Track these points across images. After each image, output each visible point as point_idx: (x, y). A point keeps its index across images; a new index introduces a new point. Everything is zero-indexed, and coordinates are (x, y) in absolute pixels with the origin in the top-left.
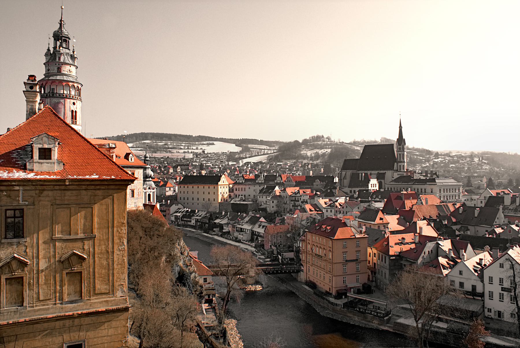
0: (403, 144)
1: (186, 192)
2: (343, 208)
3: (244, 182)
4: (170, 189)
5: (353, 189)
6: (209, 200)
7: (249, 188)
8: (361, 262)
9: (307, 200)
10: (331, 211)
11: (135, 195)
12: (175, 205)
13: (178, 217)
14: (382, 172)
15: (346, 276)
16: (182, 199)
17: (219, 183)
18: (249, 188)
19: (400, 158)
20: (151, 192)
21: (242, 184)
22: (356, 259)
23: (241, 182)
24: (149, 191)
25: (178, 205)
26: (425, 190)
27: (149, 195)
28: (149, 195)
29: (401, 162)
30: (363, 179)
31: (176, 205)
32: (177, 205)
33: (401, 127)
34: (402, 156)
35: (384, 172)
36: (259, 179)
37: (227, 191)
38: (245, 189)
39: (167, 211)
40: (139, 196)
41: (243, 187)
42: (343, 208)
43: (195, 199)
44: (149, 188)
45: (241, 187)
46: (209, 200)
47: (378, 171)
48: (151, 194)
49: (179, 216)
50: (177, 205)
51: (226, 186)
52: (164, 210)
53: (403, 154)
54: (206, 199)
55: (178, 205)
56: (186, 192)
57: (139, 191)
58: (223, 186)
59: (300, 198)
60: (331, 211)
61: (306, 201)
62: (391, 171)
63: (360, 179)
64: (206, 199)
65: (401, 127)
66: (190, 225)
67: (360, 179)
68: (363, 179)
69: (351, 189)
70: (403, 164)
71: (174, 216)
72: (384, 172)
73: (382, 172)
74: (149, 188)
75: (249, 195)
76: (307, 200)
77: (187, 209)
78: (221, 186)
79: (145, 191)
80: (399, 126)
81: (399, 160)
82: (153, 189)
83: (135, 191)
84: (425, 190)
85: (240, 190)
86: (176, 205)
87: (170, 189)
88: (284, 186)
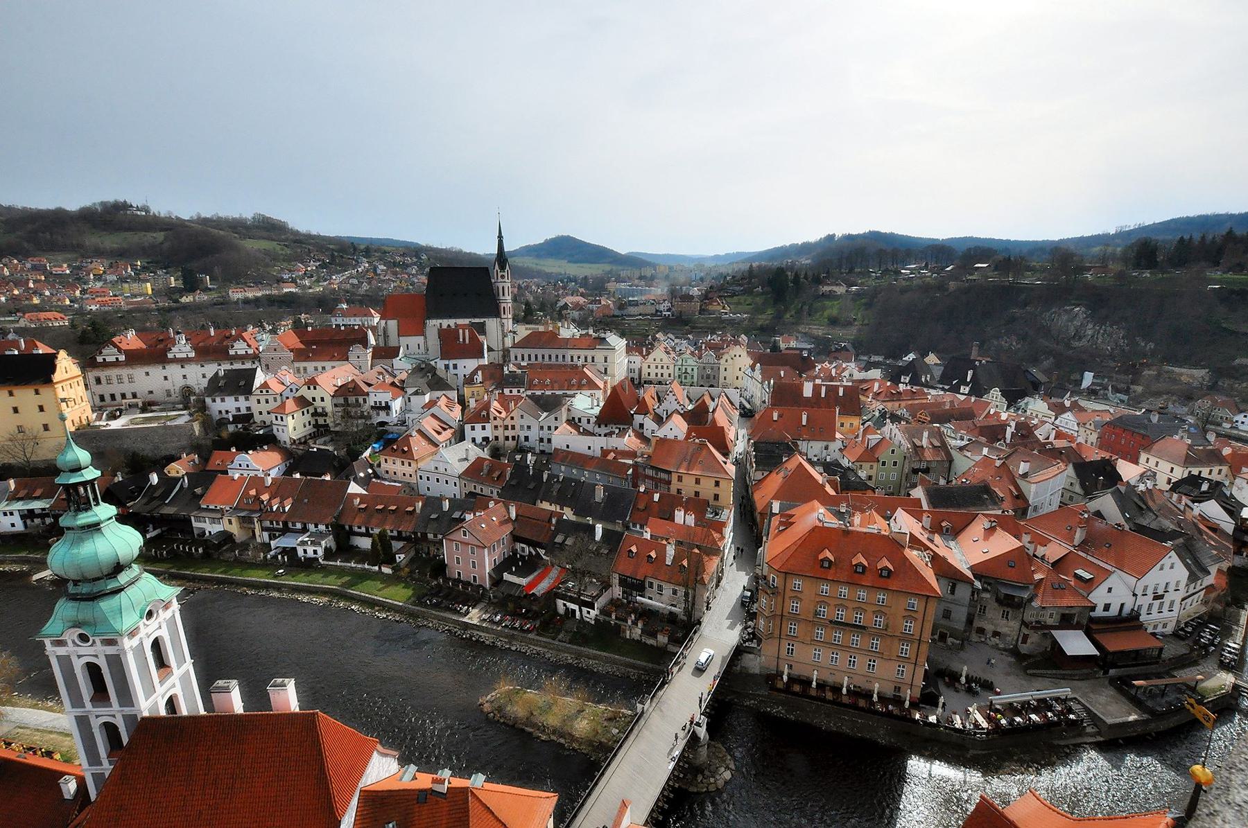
3: (122, 358)
5: (451, 363)
9: (387, 403)
10: (484, 428)
14: (477, 320)
17: (57, 377)
18: (147, 374)
21: (117, 364)
23: (112, 359)
26: (593, 358)
30: (467, 341)
33: (500, 237)
35: (482, 320)
36: (174, 349)
41: (124, 372)
42: (512, 418)
47: (470, 320)
51: (75, 380)
58: (68, 382)
59: (365, 401)
61: (383, 405)
63: (461, 340)
65: (500, 237)
67: (461, 340)
68: (467, 341)
69: (447, 362)
72: (482, 320)
73: (477, 320)
75: (151, 392)
76: (387, 403)
84: (593, 358)
88: (260, 361)
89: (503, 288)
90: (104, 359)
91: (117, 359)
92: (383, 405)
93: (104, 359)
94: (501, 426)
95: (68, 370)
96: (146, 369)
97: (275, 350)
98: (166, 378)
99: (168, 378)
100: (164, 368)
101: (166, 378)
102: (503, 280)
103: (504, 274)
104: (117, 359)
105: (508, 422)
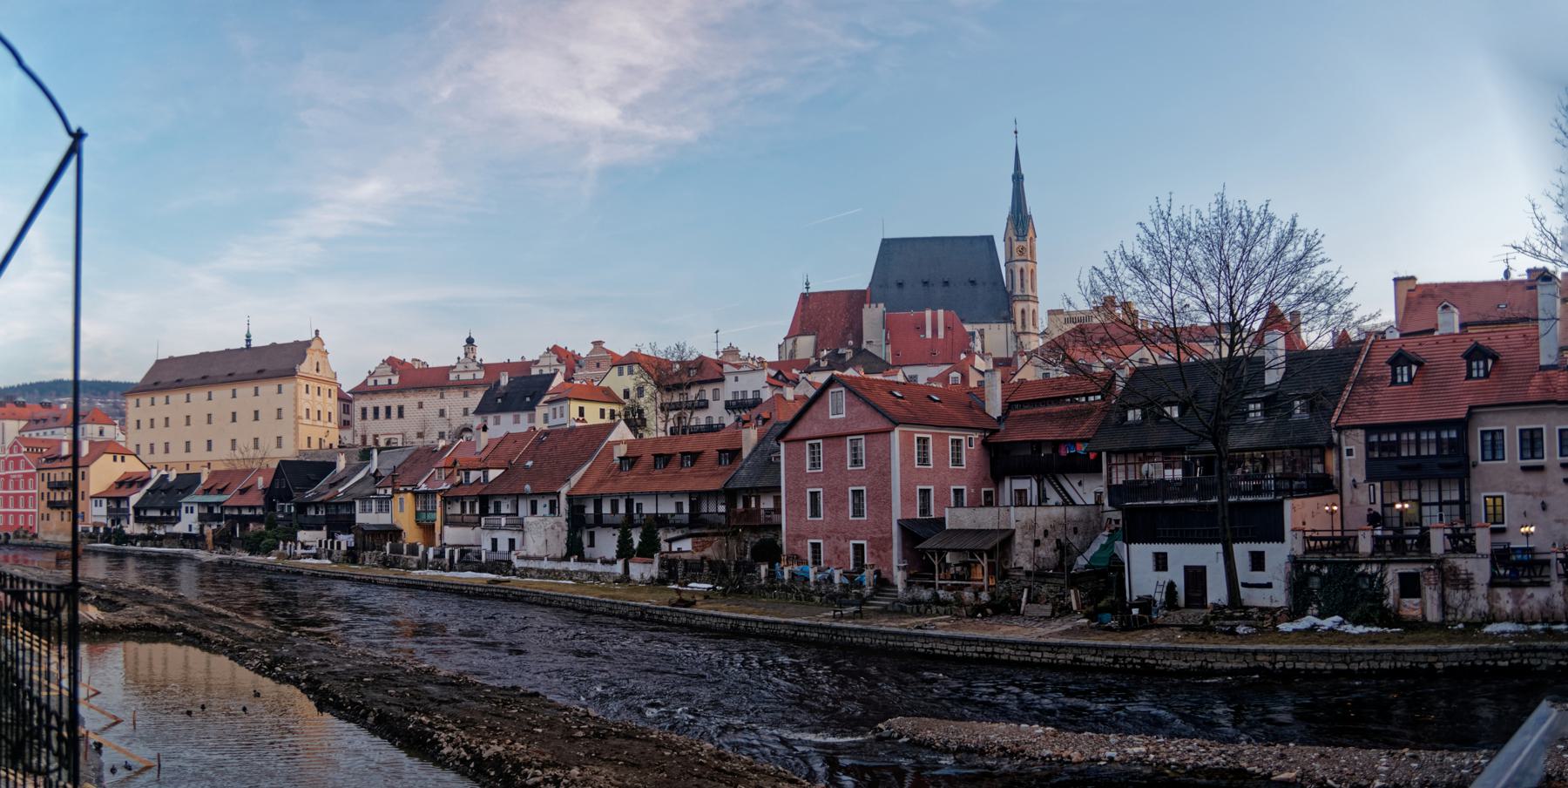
0: (1030, 234)
6: (256, 447)
7: (421, 406)
12: (111, 456)
18: (421, 406)
19: (1022, 285)
25: (123, 460)
29: (1026, 299)
31: (115, 459)
32: (119, 457)
33: (1018, 178)
34: (1028, 277)
38: (401, 409)
41: (394, 401)
45: (382, 402)
46: (256, 447)
50: (119, 457)
53: (1032, 271)
54: (245, 442)
55: (123, 460)
58: (317, 385)
62: (1003, 326)
64: (245, 442)
65: (1018, 178)
70: (1032, 306)
77: (164, 472)
78: (311, 384)
80: (1012, 171)
81: (1020, 293)
85: (382, 413)
86: (115, 459)
89: (1022, 271)
90: (376, 381)
91: (390, 380)
93: (376, 381)
95: (320, 368)
96: (421, 397)
100: (442, 397)
102: (1023, 258)
103: (1023, 244)
104: (390, 380)
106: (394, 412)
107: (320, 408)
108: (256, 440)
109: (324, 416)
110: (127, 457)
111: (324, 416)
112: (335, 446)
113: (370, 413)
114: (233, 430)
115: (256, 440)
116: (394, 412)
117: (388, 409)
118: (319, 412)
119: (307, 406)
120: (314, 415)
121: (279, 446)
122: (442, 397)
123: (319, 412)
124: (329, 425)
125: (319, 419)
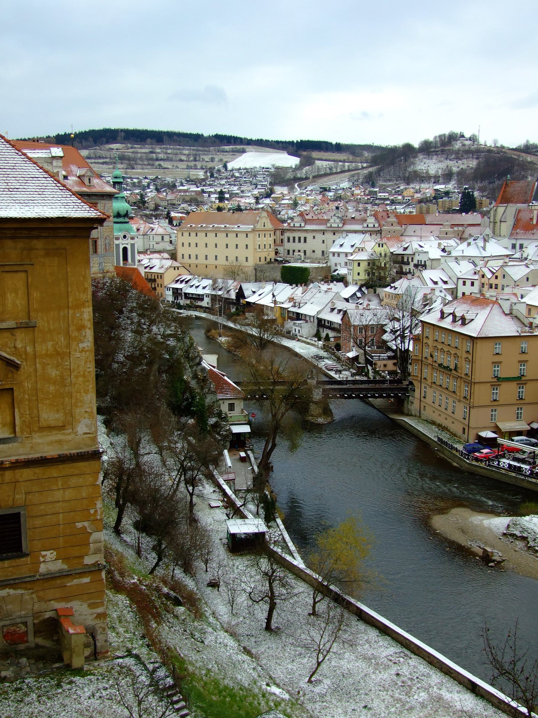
1: (192, 245)
2: (496, 277)
4: (163, 239)
6: (237, 260)
7: (314, 237)
8: (528, 382)
9: (425, 261)
10: (472, 284)
11: (99, 250)
13: (179, 291)
15: (524, 407)
16: (187, 257)
18: (314, 237)
20: (127, 244)
22: (518, 377)
24: (125, 241)
25: (178, 269)
27: (125, 250)
28: (125, 250)
32: (176, 268)
37: (270, 243)
38: (305, 239)
39: (157, 280)
40: (106, 252)
42: (496, 277)
43: (211, 258)
44: (125, 237)
45: (297, 235)
46: (237, 260)
48: (129, 247)
49: (181, 289)
50: (176, 268)
51: (269, 233)
52: (153, 278)
55: (178, 269)
56: (192, 245)
57: (107, 241)
58: (264, 233)
59: (412, 259)
60: (472, 284)
61: (423, 263)
64: (232, 258)
66: (201, 307)
71: (171, 290)
74: (125, 237)
75: (314, 251)
78: (261, 233)
79: (116, 242)
82: (132, 238)
83: (99, 243)
86: (175, 269)
87: (163, 239)
88: (381, 233)
92: (423, 263)
94: (487, 284)
95: (266, 225)
97: (392, 225)
98: (323, 242)
99: (325, 242)
100: (324, 234)
101: (323, 242)
105: (494, 281)
106: (302, 240)
107: (265, 243)
108: (237, 257)
109: (267, 246)
110: (179, 268)
111: (267, 246)
112: (273, 260)
113: (291, 240)
114: (227, 252)
115: (237, 257)
116: (302, 240)
117: (300, 238)
118: (265, 245)
119: (259, 243)
120: (262, 247)
121: (247, 261)
122: (324, 234)
123: (265, 245)
124: (270, 250)
125: (265, 248)
